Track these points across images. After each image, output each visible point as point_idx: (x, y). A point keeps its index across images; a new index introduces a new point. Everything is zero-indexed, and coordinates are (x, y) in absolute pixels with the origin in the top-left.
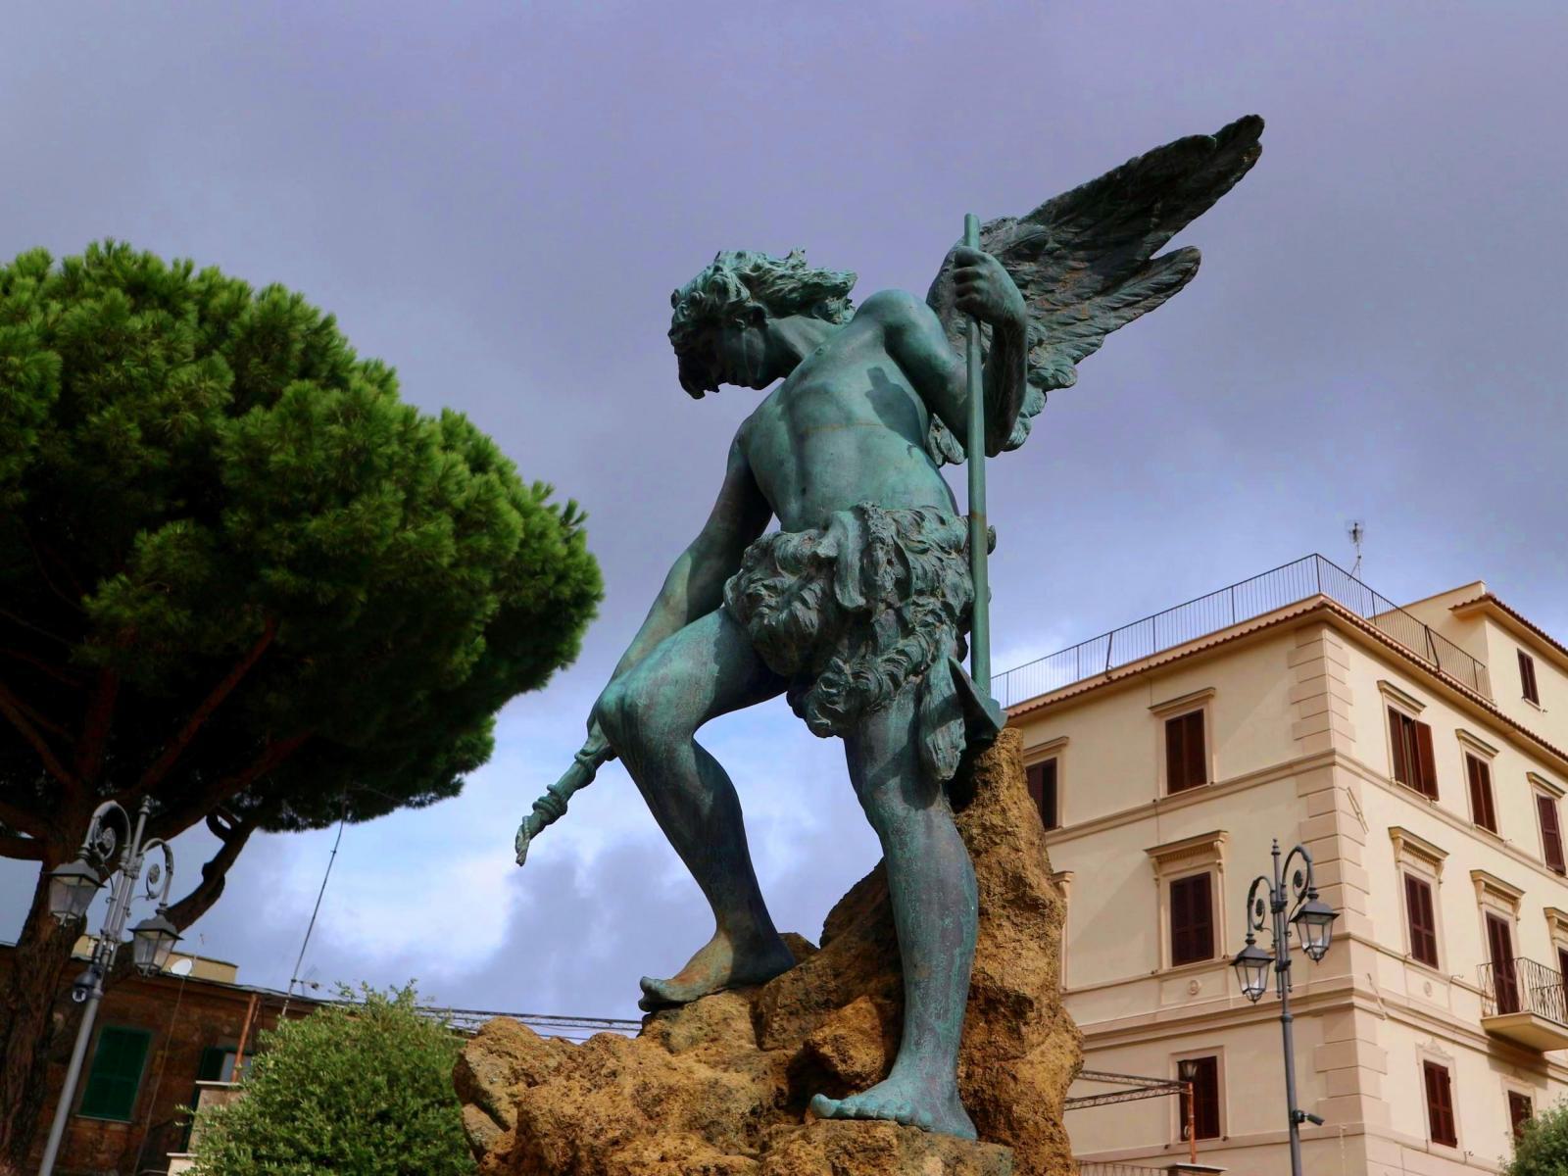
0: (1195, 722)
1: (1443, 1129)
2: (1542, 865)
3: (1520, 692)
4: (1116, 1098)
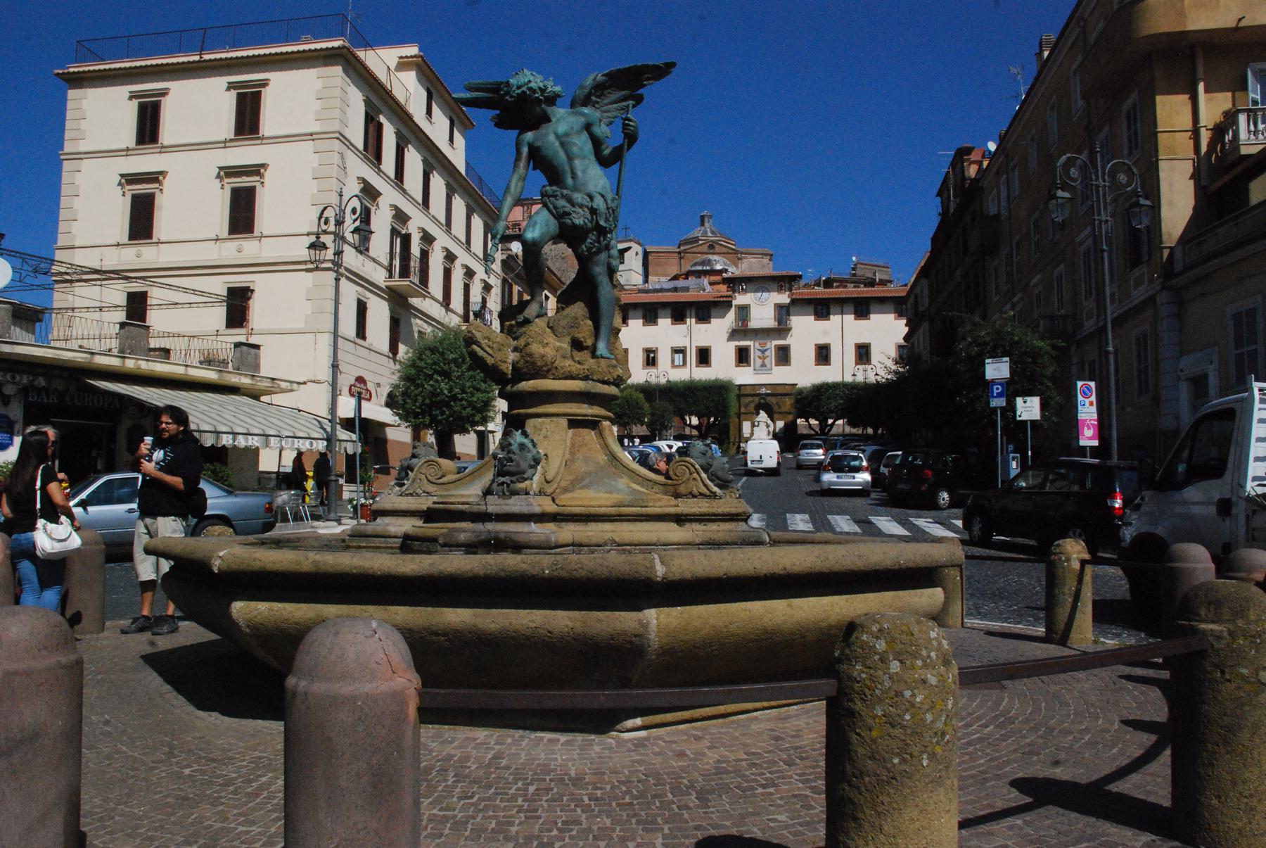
0: (257, 96)
1: (361, 331)
4: (204, 305)
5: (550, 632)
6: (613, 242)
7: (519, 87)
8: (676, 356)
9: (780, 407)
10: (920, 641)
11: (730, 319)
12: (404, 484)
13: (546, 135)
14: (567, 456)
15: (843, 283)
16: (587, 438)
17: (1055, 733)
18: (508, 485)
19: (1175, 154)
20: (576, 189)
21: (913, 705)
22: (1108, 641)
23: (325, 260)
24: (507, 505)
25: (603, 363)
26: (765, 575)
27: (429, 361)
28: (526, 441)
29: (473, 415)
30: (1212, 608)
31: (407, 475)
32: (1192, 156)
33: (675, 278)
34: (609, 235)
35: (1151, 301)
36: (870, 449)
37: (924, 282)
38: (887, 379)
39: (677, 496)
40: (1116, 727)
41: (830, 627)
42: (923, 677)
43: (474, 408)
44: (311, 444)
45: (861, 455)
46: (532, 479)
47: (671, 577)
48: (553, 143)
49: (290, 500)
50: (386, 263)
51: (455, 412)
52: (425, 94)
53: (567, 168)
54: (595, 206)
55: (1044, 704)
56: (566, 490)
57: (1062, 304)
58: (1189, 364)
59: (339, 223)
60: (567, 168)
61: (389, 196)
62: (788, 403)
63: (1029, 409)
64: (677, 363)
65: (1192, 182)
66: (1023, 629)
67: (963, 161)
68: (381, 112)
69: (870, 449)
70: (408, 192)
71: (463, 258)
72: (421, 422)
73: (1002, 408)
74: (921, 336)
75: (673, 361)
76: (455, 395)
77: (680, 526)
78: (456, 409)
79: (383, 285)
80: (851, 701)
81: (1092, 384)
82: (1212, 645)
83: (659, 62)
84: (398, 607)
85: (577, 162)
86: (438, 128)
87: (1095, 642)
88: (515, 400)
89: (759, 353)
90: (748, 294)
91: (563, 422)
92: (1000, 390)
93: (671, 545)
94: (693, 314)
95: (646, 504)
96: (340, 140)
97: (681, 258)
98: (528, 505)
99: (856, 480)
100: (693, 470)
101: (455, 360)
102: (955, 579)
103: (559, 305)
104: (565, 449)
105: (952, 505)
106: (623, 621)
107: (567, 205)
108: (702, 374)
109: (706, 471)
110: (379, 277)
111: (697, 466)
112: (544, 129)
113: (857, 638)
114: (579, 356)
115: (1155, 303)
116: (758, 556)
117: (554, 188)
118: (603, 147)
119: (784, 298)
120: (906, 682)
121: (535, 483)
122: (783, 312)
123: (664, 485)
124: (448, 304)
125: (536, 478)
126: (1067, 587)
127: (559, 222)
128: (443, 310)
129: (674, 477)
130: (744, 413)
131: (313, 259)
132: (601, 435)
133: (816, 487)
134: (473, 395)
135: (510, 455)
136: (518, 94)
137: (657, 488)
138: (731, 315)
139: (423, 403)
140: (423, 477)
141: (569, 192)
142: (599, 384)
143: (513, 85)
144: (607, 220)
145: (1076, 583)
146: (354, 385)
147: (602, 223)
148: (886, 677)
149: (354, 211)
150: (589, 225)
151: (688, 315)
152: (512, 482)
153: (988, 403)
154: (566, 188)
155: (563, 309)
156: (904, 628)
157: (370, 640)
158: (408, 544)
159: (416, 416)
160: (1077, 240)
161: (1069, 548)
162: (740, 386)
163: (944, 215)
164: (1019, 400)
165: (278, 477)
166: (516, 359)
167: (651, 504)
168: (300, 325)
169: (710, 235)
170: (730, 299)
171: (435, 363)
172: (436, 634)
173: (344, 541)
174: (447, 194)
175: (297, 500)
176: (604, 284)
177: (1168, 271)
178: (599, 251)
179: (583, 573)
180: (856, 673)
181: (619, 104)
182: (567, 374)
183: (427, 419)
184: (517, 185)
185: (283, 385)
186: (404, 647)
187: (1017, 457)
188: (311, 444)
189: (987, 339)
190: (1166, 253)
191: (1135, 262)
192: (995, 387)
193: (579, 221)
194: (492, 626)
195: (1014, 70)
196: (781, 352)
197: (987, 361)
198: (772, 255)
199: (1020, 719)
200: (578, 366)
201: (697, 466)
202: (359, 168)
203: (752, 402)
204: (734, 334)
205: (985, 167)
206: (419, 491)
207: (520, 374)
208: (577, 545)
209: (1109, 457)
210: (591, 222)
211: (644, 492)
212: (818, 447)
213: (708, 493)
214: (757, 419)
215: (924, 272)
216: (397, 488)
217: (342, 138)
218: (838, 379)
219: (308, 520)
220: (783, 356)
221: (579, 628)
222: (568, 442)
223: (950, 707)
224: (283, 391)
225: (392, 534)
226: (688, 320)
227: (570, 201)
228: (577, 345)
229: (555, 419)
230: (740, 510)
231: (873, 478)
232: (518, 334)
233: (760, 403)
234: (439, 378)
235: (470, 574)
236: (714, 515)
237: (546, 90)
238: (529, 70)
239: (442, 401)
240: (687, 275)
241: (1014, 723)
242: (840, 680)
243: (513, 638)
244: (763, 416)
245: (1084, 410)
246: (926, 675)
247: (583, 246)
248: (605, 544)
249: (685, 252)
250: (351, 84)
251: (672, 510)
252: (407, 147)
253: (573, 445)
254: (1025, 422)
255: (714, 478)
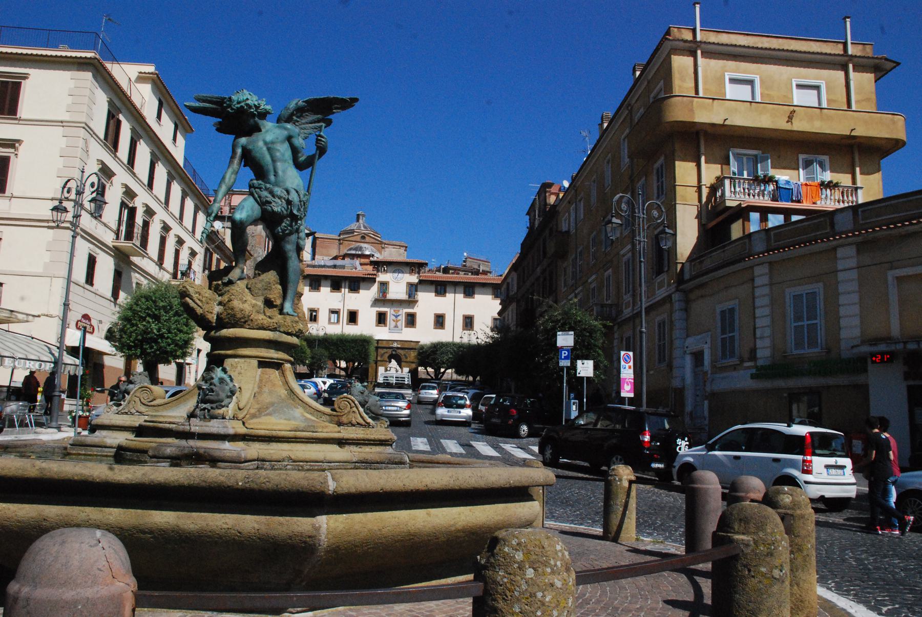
1: (90, 279)
2: (145, 186)
3: (156, 116)
5: (240, 533)
6: (302, 227)
7: (239, 103)
8: (333, 315)
9: (406, 358)
10: (549, 553)
11: (374, 291)
12: (121, 405)
13: (258, 141)
14: (256, 389)
15: (456, 270)
16: (272, 376)
17: (619, 612)
18: (209, 411)
19: (686, 201)
20: (276, 184)
21: (543, 604)
22: (645, 539)
23: (65, 221)
24: (206, 426)
25: (288, 317)
26: (412, 490)
27: (144, 307)
28: (225, 376)
29: (176, 351)
30: (742, 524)
31: (124, 397)
32: (697, 203)
33: (335, 258)
34: (299, 222)
35: (669, 297)
36: (472, 392)
37: (514, 275)
38: (486, 342)
39: (340, 424)
40: (661, 606)
41: (459, 531)
42: (551, 581)
43: (177, 345)
44: (41, 365)
45: (465, 396)
46: (228, 407)
47: (340, 491)
48: (261, 148)
49: (18, 409)
50: (115, 227)
51: (161, 347)
52: (157, 103)
53: (271, 168)
54: (290, 199)
55: (608, 588)
56: (254, 416)
57: (609, 296)
58: (693, 343)
59: (79, 193)
60: (271, 168)
61: (121, 177)
62: (413, 355)
63: (585, 368)
64: (332, 321)
65: (697, 220)
66: (586, 529)
67: (546, 192)
68: (121, 112)
69: (472, 392)
70: (137, 175)
71: (176, 229)
72: (134, 354)
73: (567, 367)
74: (510, 313)
75: (330, 319)
76: (162, 334)
77: (341, 447)
78: (162, 345)
79: (111, 245)
80: (495, 600)
81: (631, 354)
82: (743, 551)
83: (346, 97)
84: (112, 509)
85: (279, 164)
86: (165, 129)
87: (637, 539)
88: (216, 343)
89: (394, 318)
90: (388, 274)
91: (255, 362)
92: (566, 355)
93: (334, 462)
94: (347, 284)
95: (316, 430)
96: (86, 130)
97: (340, 244)
98: (224, 427)
99: (461, 414)
100: (353, 405)
101: (164, 308)
102: (538, 492)
103: (257, 272)
104: (254, 384)
105: (530, 435)
106: (300, 525)
107: (269, 195)
108: (352, 330)
109: (363, 406)
110: (109, 238)
111: (356, 402)
112: (256, 136)
113: (500, 550)
114: (269, 312)
115: (671, 300)
116: (406, 476)
117: (260, 182)
118: (300, 155)
119: (414, 279)
120: (538, 585)
121: (230, 410)
122: (413, 289)
123: (330, 415)
124: (162, 264)
125: (231, 406)
126: (620, 500)
127: (262, 208)
128: (157, 268)
129: (338, 410)
130: (380, 361)
131: (55, 219)
132: (283, 374)
133: (432, 418)
134: (176, 335)
135: (212, 387)
136: (237, 108)
137: (324, 418)
138: (375, 288)
139: (136, 339)
140: (137, 400)
141: (271, 186)
142: (284, 335)
143: (234, 101)
144: (299, 210)
145: (625, 497)
146: (80, 321)
147: (295, 212)
148: (523, 582)
149: (92, 185)
150: (285, 212)
151: (343, 285)
152: (212, 408)
153: (558, 363)
154: (269, 183)
155: (259, 275)
156: (537, 543)
157: (94, 549)
158: (121, 455)
159: (130, 348)
160: (622, 252)
161: (621, 471)
162: (378, 341)
163: (531, 228)
164: (579, 362)
165: (8, 391)
166: (220, 311)
167: (320, 430)
168: (39, 270)
169: (362, 228)
170: (375, 277)
171: (148, 308)
172: (143, 532)
173: (65, 448)
174: (168, 180)
175: (24, 410)
176: (293, 259)
177: (680, 279)
178: (291, 233)
179: (269, 486)
180: (499, 578)
181: (313, 125)
182: (260, 325)
183: (139, 351)
184: (230, 177)
185: (20, 316)
186: (118, 545)
187: (576, 403)
188: (41, 365)
189: (559, 317)
190: (679, 266)
191: (659, 270)
192: (563, 352)
193: (277, 209)
194: (192, 526)
195: (584, 134)
196: (409, 318)
197: (558, 333)
198: (406, 247)
199: (593, 600)
200: (269, 320)
201: (356, 402)
202: (99, 153)
203: (386, 352)
204: (377, 302)
205: (561, 197)
206: (133, 411)
207: (222, 323)
208: (261, 461)
209: (642, 406)
210: (287, 211)
211: (313, 420)
212: (434, 388)
213: (364, 423)
214: (390, 366)
215: (515, 268)
216: (115, 408)
217: (88, 128)
218: (449, 340)
219: (32, 426)
220: (411, 320)
221: (264, 530)
222: (257, 379)
223: (570, 604)
224: (19, 321)
225: (108, 445)
226: (343, 290)
227: (272, 193)
228: (269, 303)
229: (248, 360)
230: (388, 437)
231: (473, 413)
232: (223, 291)
233: (392, 353)
234: (151, 320)
235: (176, 484)
236: (368, 440)
237: (260, 107)
238: (248, 91)
239: (151, 338)
240: (344, 257)
241: (589, 604)
242: (486, 583)
243: (209, 537)
244: (394, 363)
245: (625, 372)
246: (553, 580)
247: (279, 228)
248: (283, 460)
249: (343, 239)
250: (99, 88)
251: (336, 435)
252: (139, 141)
253: (261, 381)
254: (582, 378)
255: (368, 411)
